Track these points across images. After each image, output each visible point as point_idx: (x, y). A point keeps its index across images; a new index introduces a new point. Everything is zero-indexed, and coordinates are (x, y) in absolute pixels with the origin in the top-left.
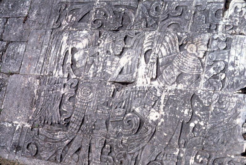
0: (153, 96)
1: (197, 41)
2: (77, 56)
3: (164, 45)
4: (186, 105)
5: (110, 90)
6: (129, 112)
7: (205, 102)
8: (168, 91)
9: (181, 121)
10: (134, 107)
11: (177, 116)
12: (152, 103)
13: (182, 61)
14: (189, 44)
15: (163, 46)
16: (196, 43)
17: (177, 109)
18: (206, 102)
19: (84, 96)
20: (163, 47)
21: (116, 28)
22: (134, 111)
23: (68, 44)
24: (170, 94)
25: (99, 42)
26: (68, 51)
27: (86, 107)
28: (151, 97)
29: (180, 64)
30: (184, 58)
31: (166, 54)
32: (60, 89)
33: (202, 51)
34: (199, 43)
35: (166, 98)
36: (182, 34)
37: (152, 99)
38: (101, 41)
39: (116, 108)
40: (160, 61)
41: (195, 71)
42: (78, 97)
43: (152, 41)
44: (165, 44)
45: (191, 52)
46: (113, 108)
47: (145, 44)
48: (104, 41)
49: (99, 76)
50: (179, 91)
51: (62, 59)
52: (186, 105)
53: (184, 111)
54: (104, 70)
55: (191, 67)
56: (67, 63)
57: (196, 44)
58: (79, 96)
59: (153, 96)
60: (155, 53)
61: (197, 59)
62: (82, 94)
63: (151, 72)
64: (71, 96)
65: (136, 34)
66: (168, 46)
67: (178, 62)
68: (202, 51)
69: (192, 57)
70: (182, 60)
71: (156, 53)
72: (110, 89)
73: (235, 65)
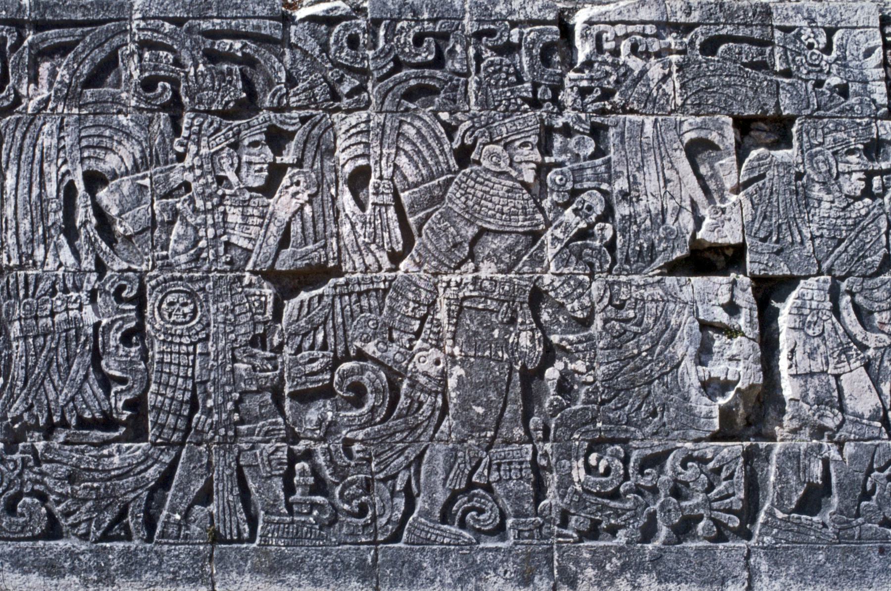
0: (411, 304)
3: (406, 153)
5: (263, 299)
6: (347, 358)
8: (453, 284)
9: (518, 368)
10: (358, 344)
11: (500, 353)
14: (484, 145)
17: (496, 333)
22: (361, 356)
24: (461, 295)
26: (72, 183)
27: (191, 357)
32: (80, 309)
33: (527, 162)
35: (453, 307)
38: (185, 146)
39: (299, 350)
40: (405, 196)
42: (153, 327)
43: (364, 140)
45: (498, 169)
46: (287, 350)
47: (343, 151)
48: (198, 144)
50: (486, 284)
52: (520, 320)
53: (518, 335)
55: (506, 209)
56: (78, 224)
58: (157, 326)
59: (411, 304)
61: (518, 185)
62: (167, 317)
63: (386, 235)
65: (303, 120)
68: (527, 162)
69: (504, 182)
72: (261, 295)
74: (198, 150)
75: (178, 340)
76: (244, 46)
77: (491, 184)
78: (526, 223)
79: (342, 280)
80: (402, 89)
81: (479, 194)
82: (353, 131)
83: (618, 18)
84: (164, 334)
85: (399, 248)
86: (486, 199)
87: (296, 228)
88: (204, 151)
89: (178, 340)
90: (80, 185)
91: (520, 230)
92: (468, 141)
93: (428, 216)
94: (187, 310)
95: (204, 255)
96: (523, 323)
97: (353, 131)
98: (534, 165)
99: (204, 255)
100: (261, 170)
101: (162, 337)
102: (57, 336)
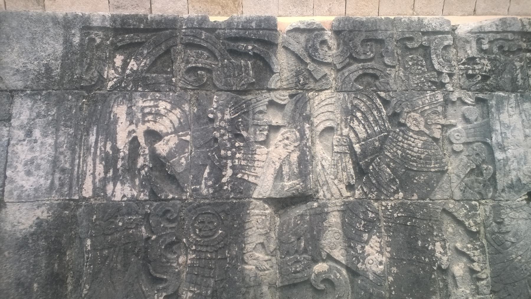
0: (363, 222)
1: (421, 107)
2: (162, 148)
3: (357, 118)
4: (435, 233)
7: (469, 224)
12: (363, 237)
13: (402, 147)
14: (408, 113)
15: (355, 119)
16: (420, 111)
18: (472, 223)
19: (203, 237)
20: (356, 123)
21: (243, 85)
22: (330, 258)
23: (131, 123)
24: (395, 215)
25: (211, 116)
28: (358, 224)
29: (399, 152)
30: (406, 142)
31: (365, 135)
34: (426, 110)
36: (389, 95)
37: (362, 229)
40: (357, 147)
41: (432, 166)
44: (359, 114)
48: (223, 114)
49: (229, 189)
51: (123, 159)
52: (435, 233)
53: (434, 245)
54: (239, 176)
55: (423, 156)
57: (421, 112)
59: (363, 222)
60: (341, 135)
61: (430, 139)
64: (168, 240)
66: (366, 118)
67: (395, 149)
70: (401, 144)
71: (344, 134)
73: (506, 149)
74: (223, 117)
75: (205, 249)
76: (254, 48)
77: (413, 140)
78: (436, 165)
79: (316, 204)
80: (353, 77)
81: (405, 146)
82: (324, 103)
83: (490, 29)
84: (195, 245)
85: (353, 182)
86: (409, 150)
87: (286, 169)
88: (227, 117)
89: (205, 249)
90: (142, 140)
91: (433, 170)
92: (398, 111)
93: (372, 160)
94: (211, 226)
95: (225, 187)
96: (437, 236)
97: (324, 103)
98: (440, 126)
99: (225, 187)
100: (263, 130)
101: (194, 248)
102: (117, 249)
